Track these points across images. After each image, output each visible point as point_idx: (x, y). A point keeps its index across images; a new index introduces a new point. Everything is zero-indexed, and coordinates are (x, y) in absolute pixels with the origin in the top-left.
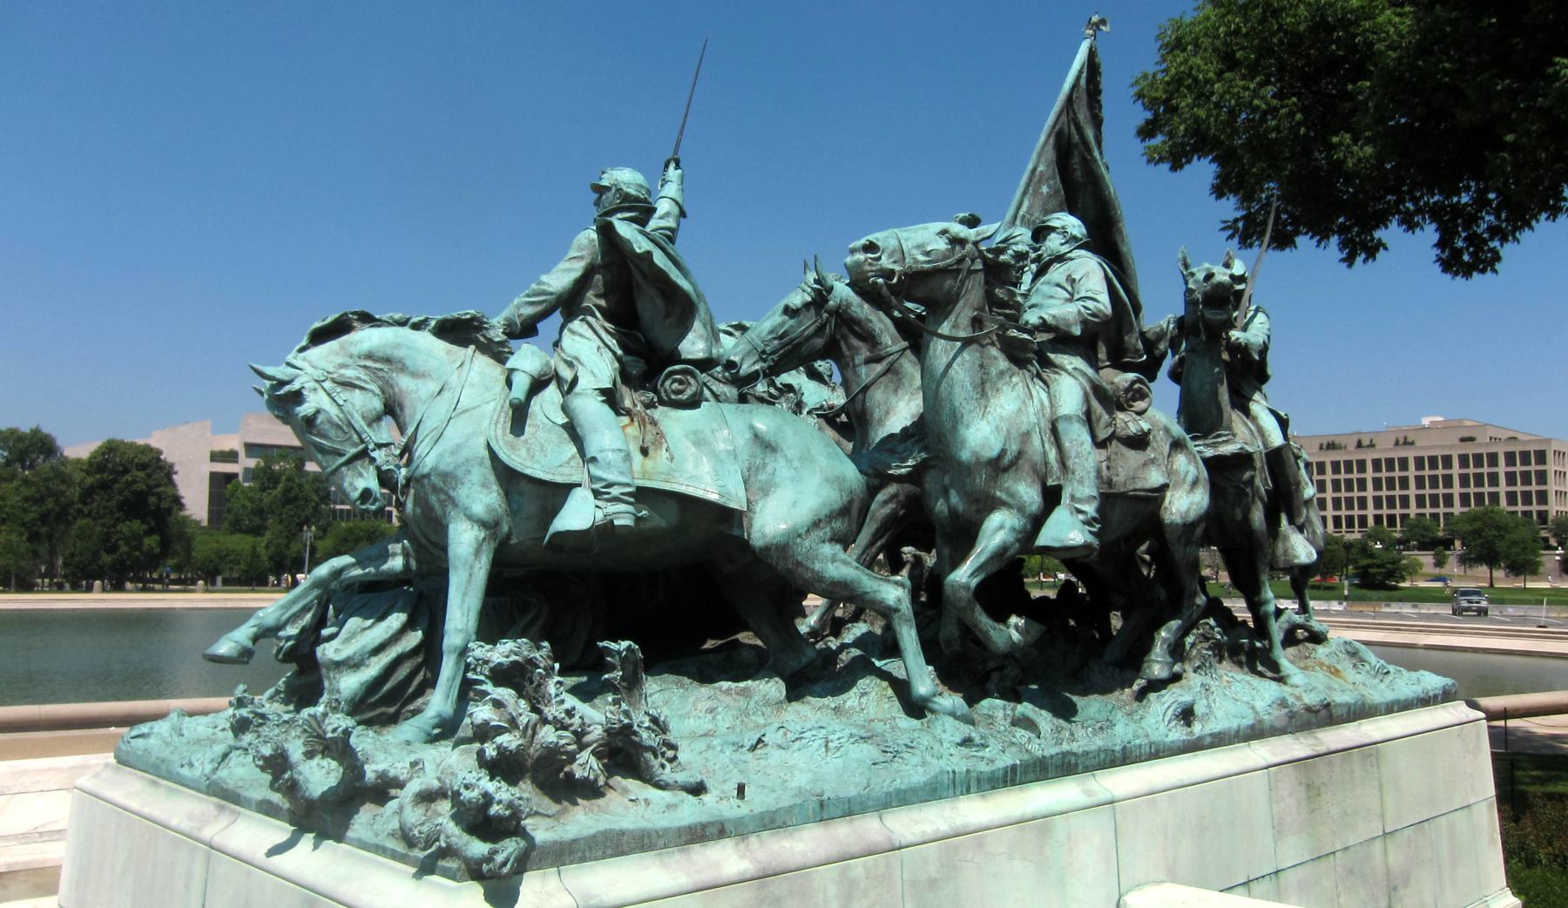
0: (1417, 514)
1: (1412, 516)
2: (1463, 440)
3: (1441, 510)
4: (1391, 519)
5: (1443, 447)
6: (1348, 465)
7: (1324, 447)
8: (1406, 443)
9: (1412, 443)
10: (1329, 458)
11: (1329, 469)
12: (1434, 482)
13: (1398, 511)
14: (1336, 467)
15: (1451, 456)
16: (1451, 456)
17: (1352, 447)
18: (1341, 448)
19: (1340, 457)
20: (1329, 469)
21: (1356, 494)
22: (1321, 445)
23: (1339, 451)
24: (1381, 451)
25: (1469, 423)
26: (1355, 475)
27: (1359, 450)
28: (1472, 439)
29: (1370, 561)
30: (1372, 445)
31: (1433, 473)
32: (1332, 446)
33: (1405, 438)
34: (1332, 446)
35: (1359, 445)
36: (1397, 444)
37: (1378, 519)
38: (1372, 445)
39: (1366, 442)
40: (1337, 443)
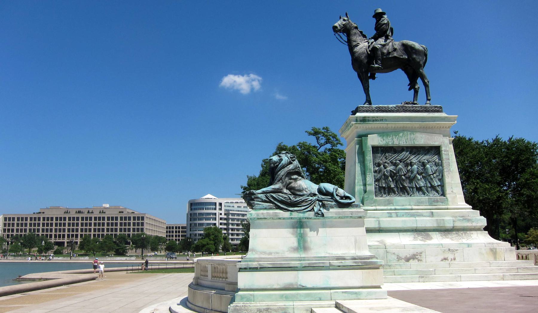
0: (107, 234)
1: (118, 234)
2: (120, 212)
3: (114, 233)
4: (99, 235)
5: (116, 214)
6: (87, 218)
7: (77, 212)
8: (103, 212)
9: (105, 213)
10: (80, 216)
11: (80, 219)
12: (99, 224)
13: (114, 233)
14: (82, 219)
15: (131, 217)
16: (131, 217)
17: (86, 213)
18: (82, 213)
19: (84, 216)
20: (80, 219)
21: (75, 227)
22: (76, 211)
23: (82, 214)
24: (96, 214)
25: (121, 207)
26: (76, 222)
27: (89, 214)
28: (122, 212)
29: (119, 247)
30: (92, 213)
31: (112, 222)
32: (79, 212)
33: (103, 211)
34: (79, 212)
35: (88, 212)
36: (100, 212)
37: (94, 235)
38: (92, 213)
39: (90, 211)
40: (81, 211)
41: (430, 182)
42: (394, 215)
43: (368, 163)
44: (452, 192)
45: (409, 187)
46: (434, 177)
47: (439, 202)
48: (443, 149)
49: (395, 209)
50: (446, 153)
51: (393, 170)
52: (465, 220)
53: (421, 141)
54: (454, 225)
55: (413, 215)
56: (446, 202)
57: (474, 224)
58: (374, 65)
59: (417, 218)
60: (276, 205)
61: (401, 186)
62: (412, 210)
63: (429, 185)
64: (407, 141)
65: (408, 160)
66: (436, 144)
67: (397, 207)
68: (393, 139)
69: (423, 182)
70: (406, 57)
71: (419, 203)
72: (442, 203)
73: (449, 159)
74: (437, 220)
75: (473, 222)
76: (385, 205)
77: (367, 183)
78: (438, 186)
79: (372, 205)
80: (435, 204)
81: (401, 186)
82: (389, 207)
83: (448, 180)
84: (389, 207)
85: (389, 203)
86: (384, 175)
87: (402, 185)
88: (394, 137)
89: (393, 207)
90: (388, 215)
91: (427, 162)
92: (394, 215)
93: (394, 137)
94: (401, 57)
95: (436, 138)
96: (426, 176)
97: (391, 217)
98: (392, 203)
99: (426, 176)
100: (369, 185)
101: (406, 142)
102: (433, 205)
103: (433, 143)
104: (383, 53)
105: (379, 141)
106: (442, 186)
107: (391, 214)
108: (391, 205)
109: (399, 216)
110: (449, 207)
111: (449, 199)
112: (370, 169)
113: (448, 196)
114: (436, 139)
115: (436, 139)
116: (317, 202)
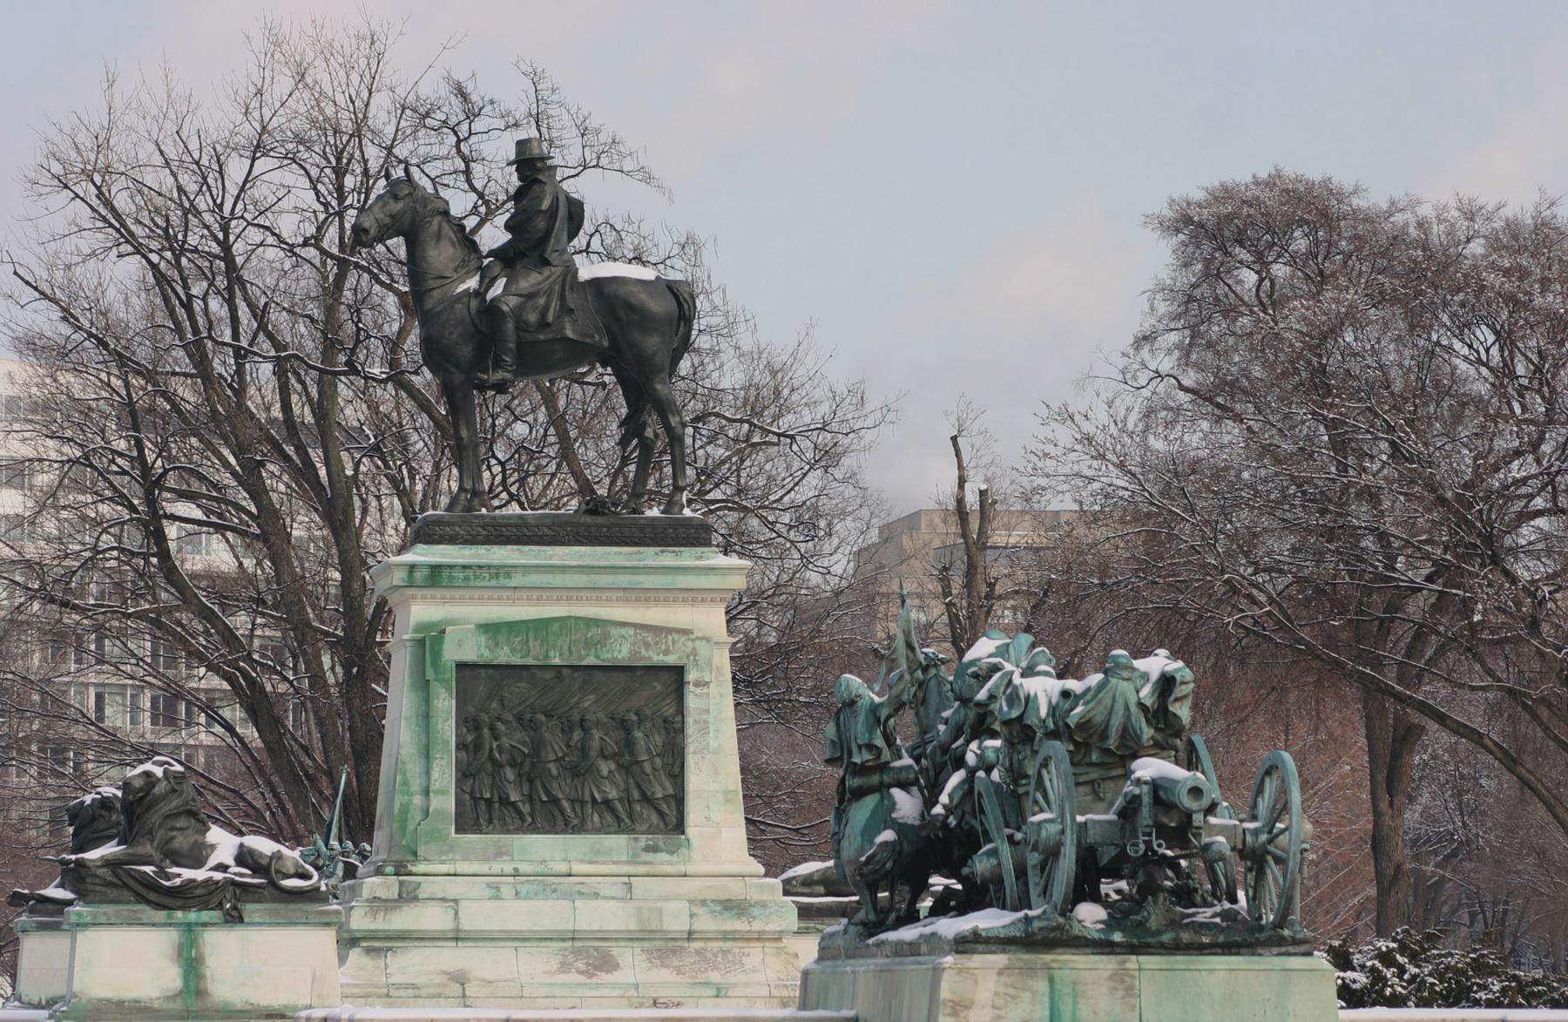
41: (639, 786)
42: (507, 892)
43: (440, 720)
44: (708, 818)
45: (572, 801)
46: (654, 769)
47: (661, 851)
48: (691, 676)
49: (516, 874)
50: (698, 691)
51: (520, 743)
52: (727, 914)
53: (620, 652)
54: (693, 928)
55: (569, 896)
56: (684, 850)
57: (757, 926)
58: (486, 371)
59: (578, 903)
60: (138, 894)
61: (545, 799)
62: (570, 875)
63: (636, 795)
64: (573, 649)
65: (576, 711)
66: (671, 660)
67: (525, 868)
68: (527, 641)
69: (617, 786)
70: (606, 344)
71: (594, 857)
72: (672, 853)
73: (708, 711)
74: (640, 909)
75: (754, 918)
76: (486, 860)
77: (432, 788)
78: (665, 798)
79: (444, 858)
80: (650, 857)
81: (545, 799)
82: (496, 867)
83: (698, 779)
84: (496, 867)
85: (499, 854)
86: (491, 758)
87: (547, 792)
88: (531, 635)
89: (509, 869)
90: (488, 893)
91: (634, 718)
92: (507, 892)
93: (531, 635)
94: (587, 340)
95: (670, 637)
96: (629, 766)
97: (497, 898)
98: (506, 854)
99: (629, 766)
100: (438, 792)
101: (570, 652)
102: (641, 859)
103: (661, 657)
104: (521, 326)
105: (479, 649)
106: (679, 799)
107: (498, 889)
108: (505, 858)
109: (522, 894)
110: (690, 869)
111: (695, 842)
112: (446, 742)
113: (691, 831)
114: (670, 643)
115: (670, 643)
116: (231, 888)
